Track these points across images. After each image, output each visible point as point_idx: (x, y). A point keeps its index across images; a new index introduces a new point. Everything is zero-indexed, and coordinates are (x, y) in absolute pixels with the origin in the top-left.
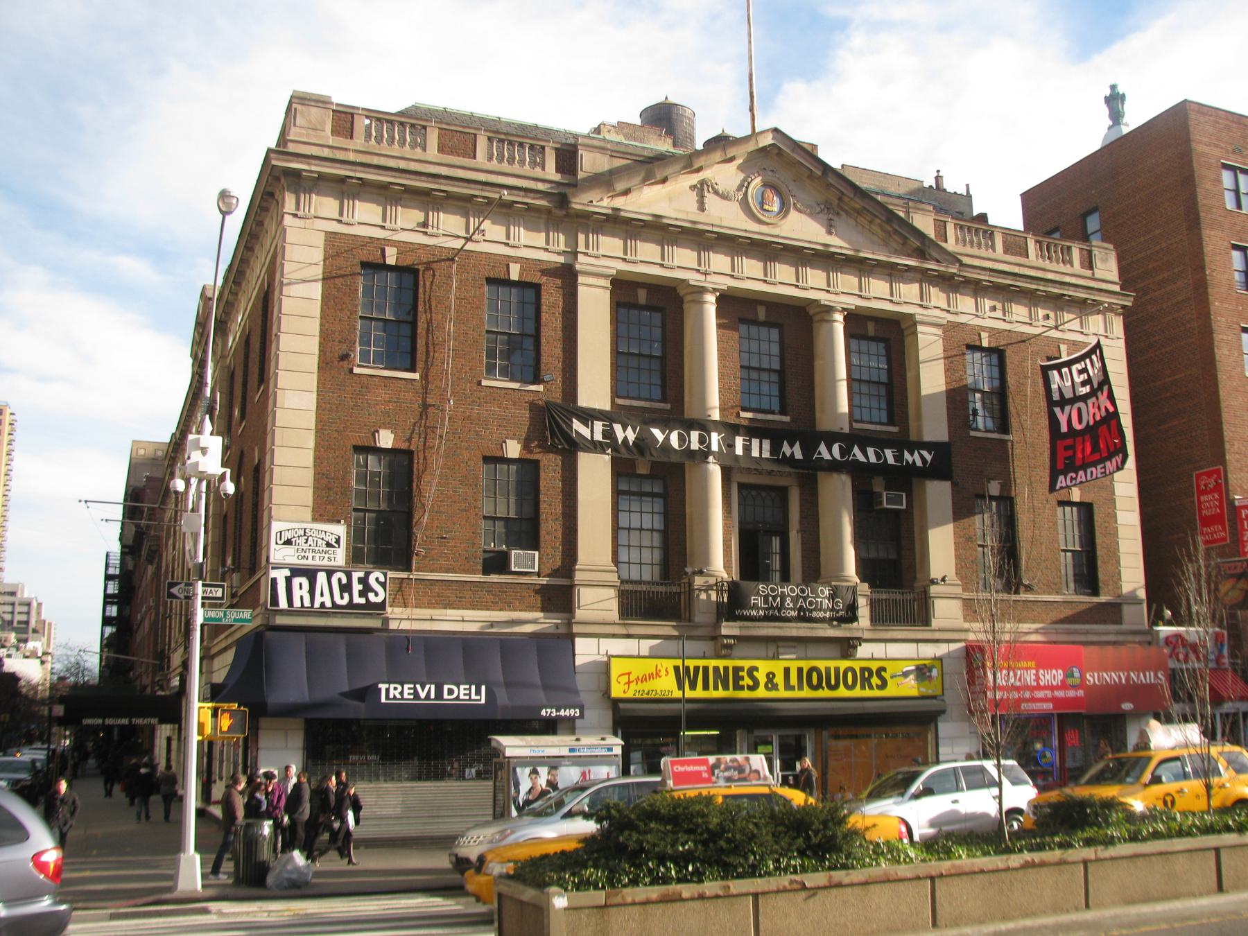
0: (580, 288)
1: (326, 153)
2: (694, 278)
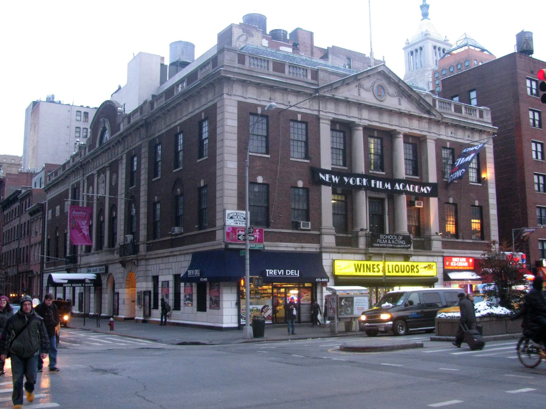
0: (321, 124)
1: (236, 70)
2: (357, 121)
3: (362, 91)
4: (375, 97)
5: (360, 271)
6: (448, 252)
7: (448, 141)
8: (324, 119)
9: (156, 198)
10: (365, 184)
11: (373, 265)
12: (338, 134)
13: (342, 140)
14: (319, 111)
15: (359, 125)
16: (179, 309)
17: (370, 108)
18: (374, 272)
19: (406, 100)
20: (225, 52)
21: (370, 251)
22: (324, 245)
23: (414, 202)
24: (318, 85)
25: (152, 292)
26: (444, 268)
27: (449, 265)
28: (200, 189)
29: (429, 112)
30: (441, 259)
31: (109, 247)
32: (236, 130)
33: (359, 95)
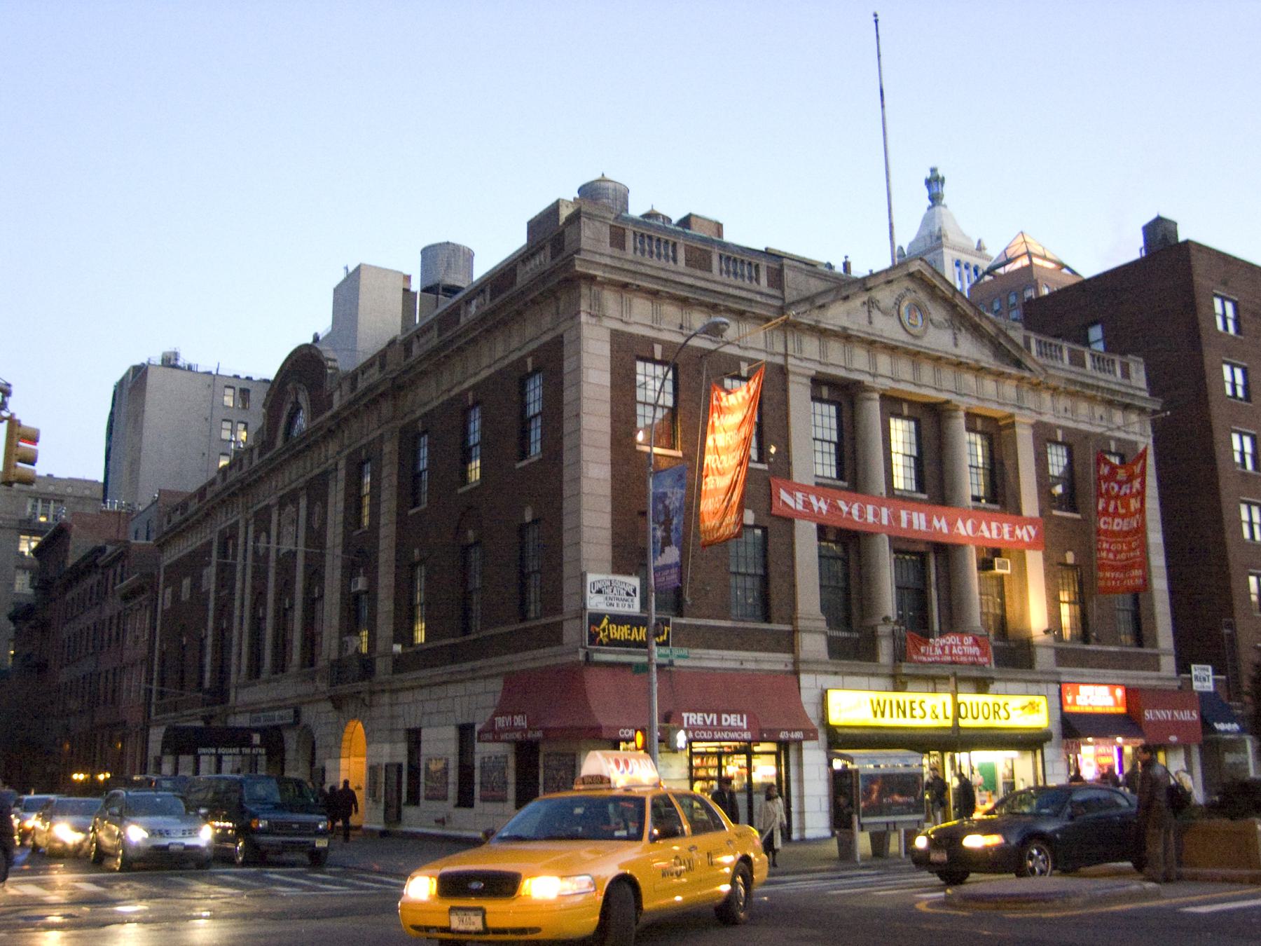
3: (875, 313)
6: (1066, 673)
7: (1059, 427)
10: (885, 522)
12: (825, 407)
13: (834, 421)
15: (872, 390)
16: (472, 806)
21: (904, 671)
22: (802, 656)
23: (992, 562)
24: (783, 299)
26: (1061, 708)
27: (1074, 703)
29: (1018, 364)
31: (303, 666)
33: (871, 323)
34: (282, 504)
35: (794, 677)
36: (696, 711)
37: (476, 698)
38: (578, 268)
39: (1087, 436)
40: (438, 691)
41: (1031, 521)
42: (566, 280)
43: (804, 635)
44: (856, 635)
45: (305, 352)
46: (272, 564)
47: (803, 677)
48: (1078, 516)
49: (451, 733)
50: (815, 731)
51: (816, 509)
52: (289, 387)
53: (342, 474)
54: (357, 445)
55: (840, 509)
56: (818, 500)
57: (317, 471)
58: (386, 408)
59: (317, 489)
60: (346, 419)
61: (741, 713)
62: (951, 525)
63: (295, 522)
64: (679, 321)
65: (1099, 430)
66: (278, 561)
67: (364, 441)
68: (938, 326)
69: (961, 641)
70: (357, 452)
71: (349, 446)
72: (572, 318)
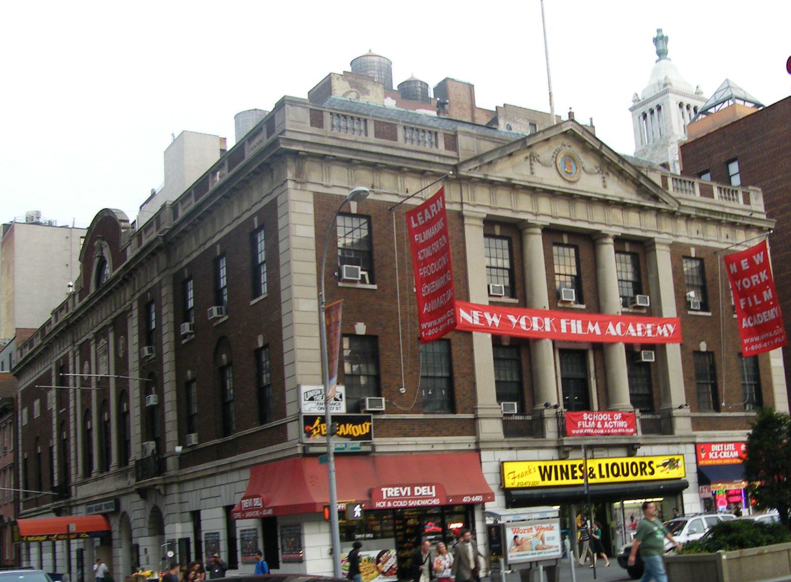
0: (466, 227)
1: (308, 138)
2: (530, 218)
3: (536, 165)
4: (561, 176)
5: (550, 479)
6: (702, 436)
8: (470, 217)
9: (189, 373)
10: (548, 329)
11: (573, 466)
14: (462, 204)
15: (534, 226)
17: (552, 194)
18: (574, 478)
19: (616, 179)
20: (287, 106)
21: (566, 443)
24: (458, 159)
25: (192, 540)
26: (697, 463)
27: (707, 457)
28: (258, 352)
29: (656, 198)
30: (691, 448)
32: (312, 244)
33: (532, 173)
34: (97, 337)
35: (477, 453)
36: (393, 486)
37: (233, 487)
38: (282, 146)
39: (715, 252)
40: (209, 482)
41: (669, 321)
42: (275, 155)
43: (483, 421)
44: (529, 418)
45: (106, 214)
46: (94, 387)
47: (483, 453)
48: (709, 314)
49: (220, 513)
50: (492, 495)
51: (490, 323)
52: (96, 243)
53: (135, 313)
54: (144, 290)
55: (510, 321)
56: (492, 316)
57: (119, 311)
58: (162, 259)
59: (119, 325)
60: (135, 269)
61: (431, 485)
62: (603, 328)
63: (106, 352)
64: (371, 182)
65: (724, 246)
66: (98, 383)
67: (149, 286)
68: (589, 173)
69: (612, 417)
70: (144, 296)
71: (139, 291)
72: (282, 185)
